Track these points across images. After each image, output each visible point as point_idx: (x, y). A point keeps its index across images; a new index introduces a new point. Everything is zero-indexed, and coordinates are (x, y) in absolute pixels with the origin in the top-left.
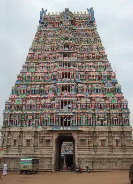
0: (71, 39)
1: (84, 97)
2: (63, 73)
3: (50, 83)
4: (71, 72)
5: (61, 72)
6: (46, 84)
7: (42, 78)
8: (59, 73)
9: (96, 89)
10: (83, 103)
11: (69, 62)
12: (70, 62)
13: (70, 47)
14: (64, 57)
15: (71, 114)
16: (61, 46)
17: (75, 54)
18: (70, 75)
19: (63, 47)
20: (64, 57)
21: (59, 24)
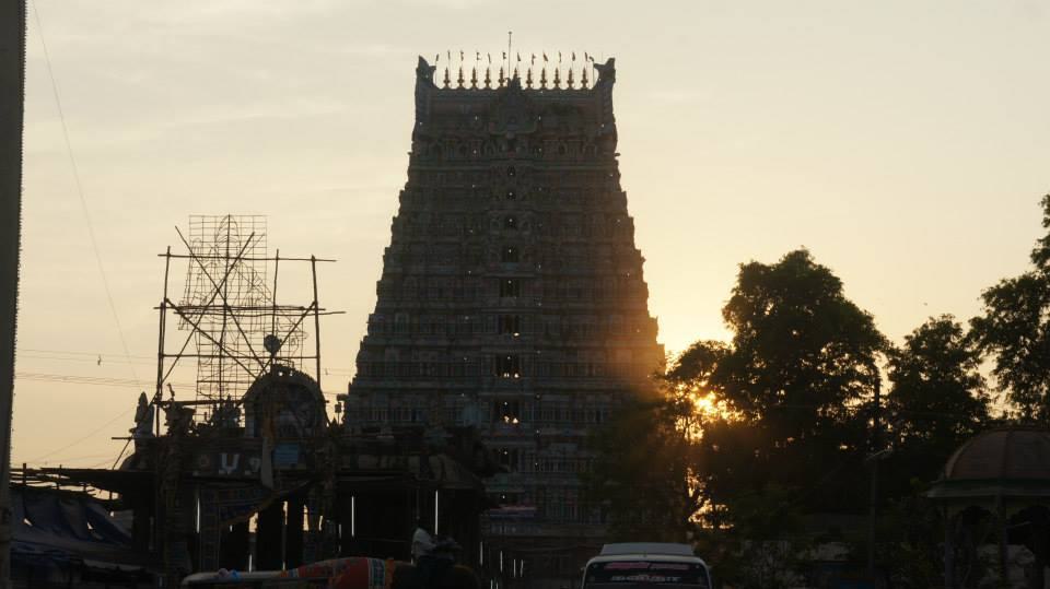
0: (526, 224)
1: (558, 439)
2: (498, 358)
3: (457, 386)
4: (523, 354)
5: (492, 354)
6: (445, 391)
7: (433, 369)
8: (488, 356)
9: (594, 411)
10: (556, 458)
11: (517, 317)
12: (521, 316)
13: (521, 257)
14: (502, 295)
15: (520, 490)
16: (491, 251)
17: (537, 284)
18: (520, 361)
19: (500, 258)
20: (502, 295)
21: (484, 143)
